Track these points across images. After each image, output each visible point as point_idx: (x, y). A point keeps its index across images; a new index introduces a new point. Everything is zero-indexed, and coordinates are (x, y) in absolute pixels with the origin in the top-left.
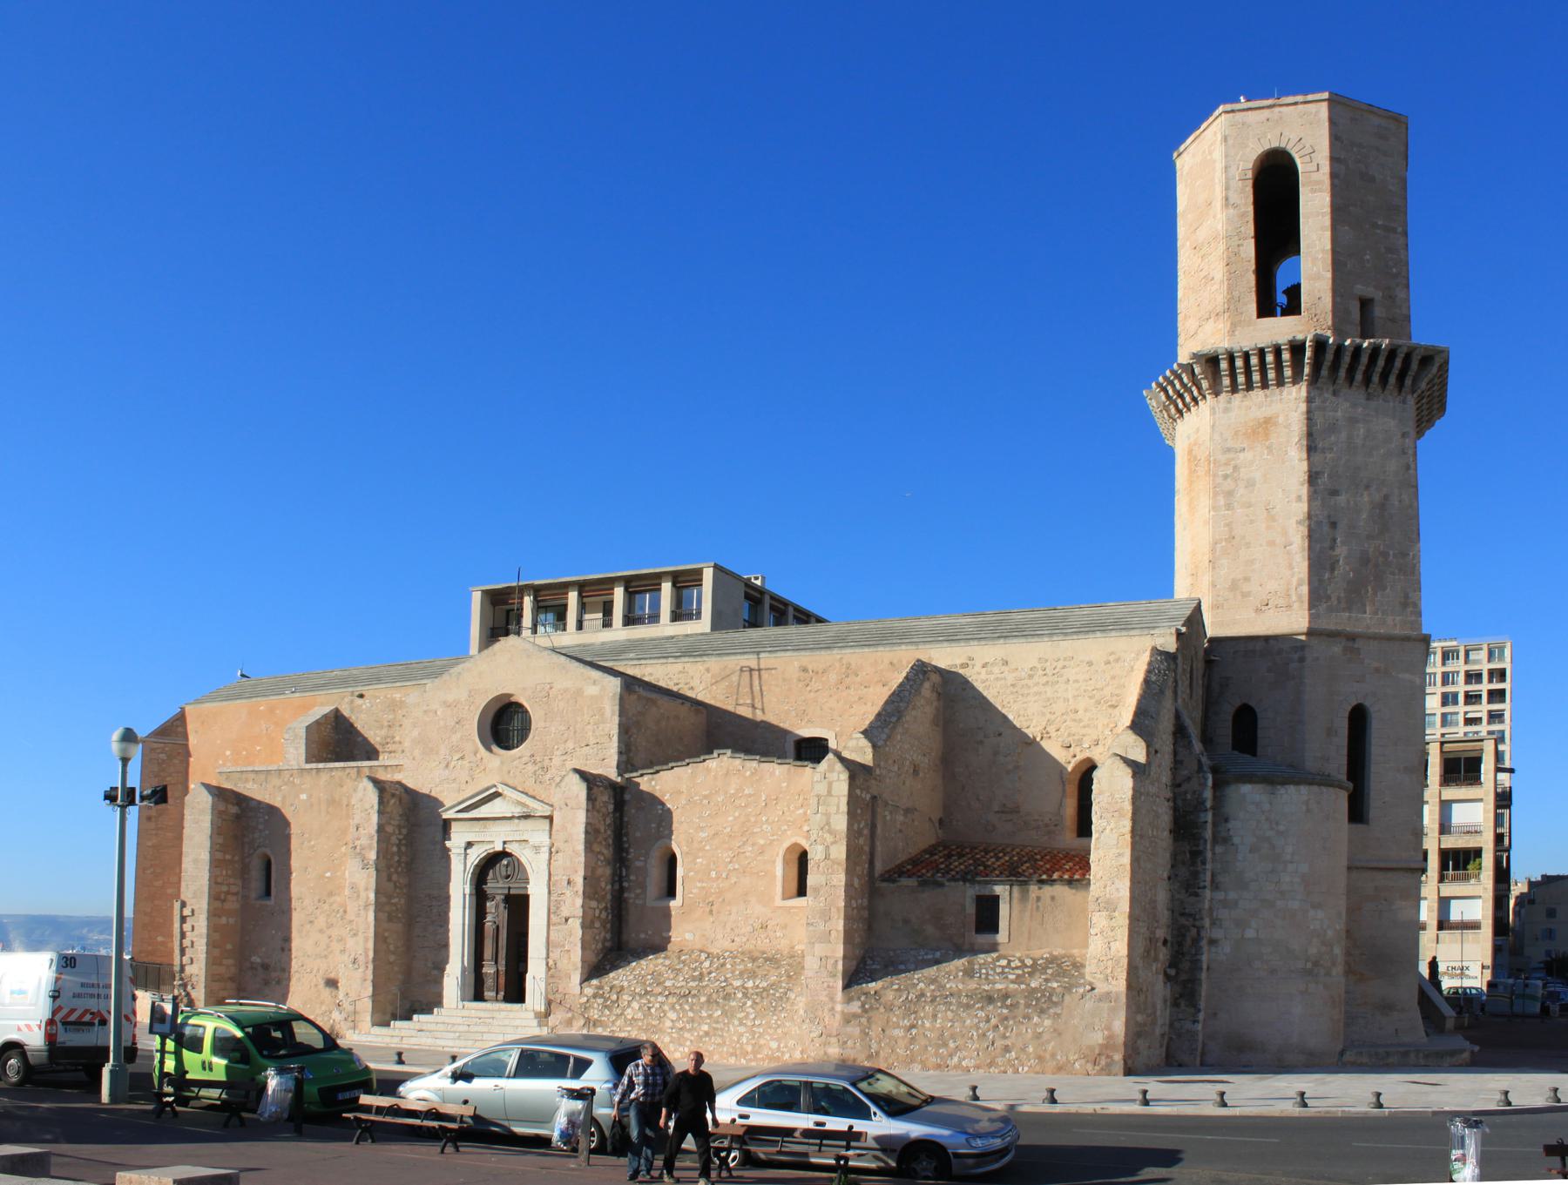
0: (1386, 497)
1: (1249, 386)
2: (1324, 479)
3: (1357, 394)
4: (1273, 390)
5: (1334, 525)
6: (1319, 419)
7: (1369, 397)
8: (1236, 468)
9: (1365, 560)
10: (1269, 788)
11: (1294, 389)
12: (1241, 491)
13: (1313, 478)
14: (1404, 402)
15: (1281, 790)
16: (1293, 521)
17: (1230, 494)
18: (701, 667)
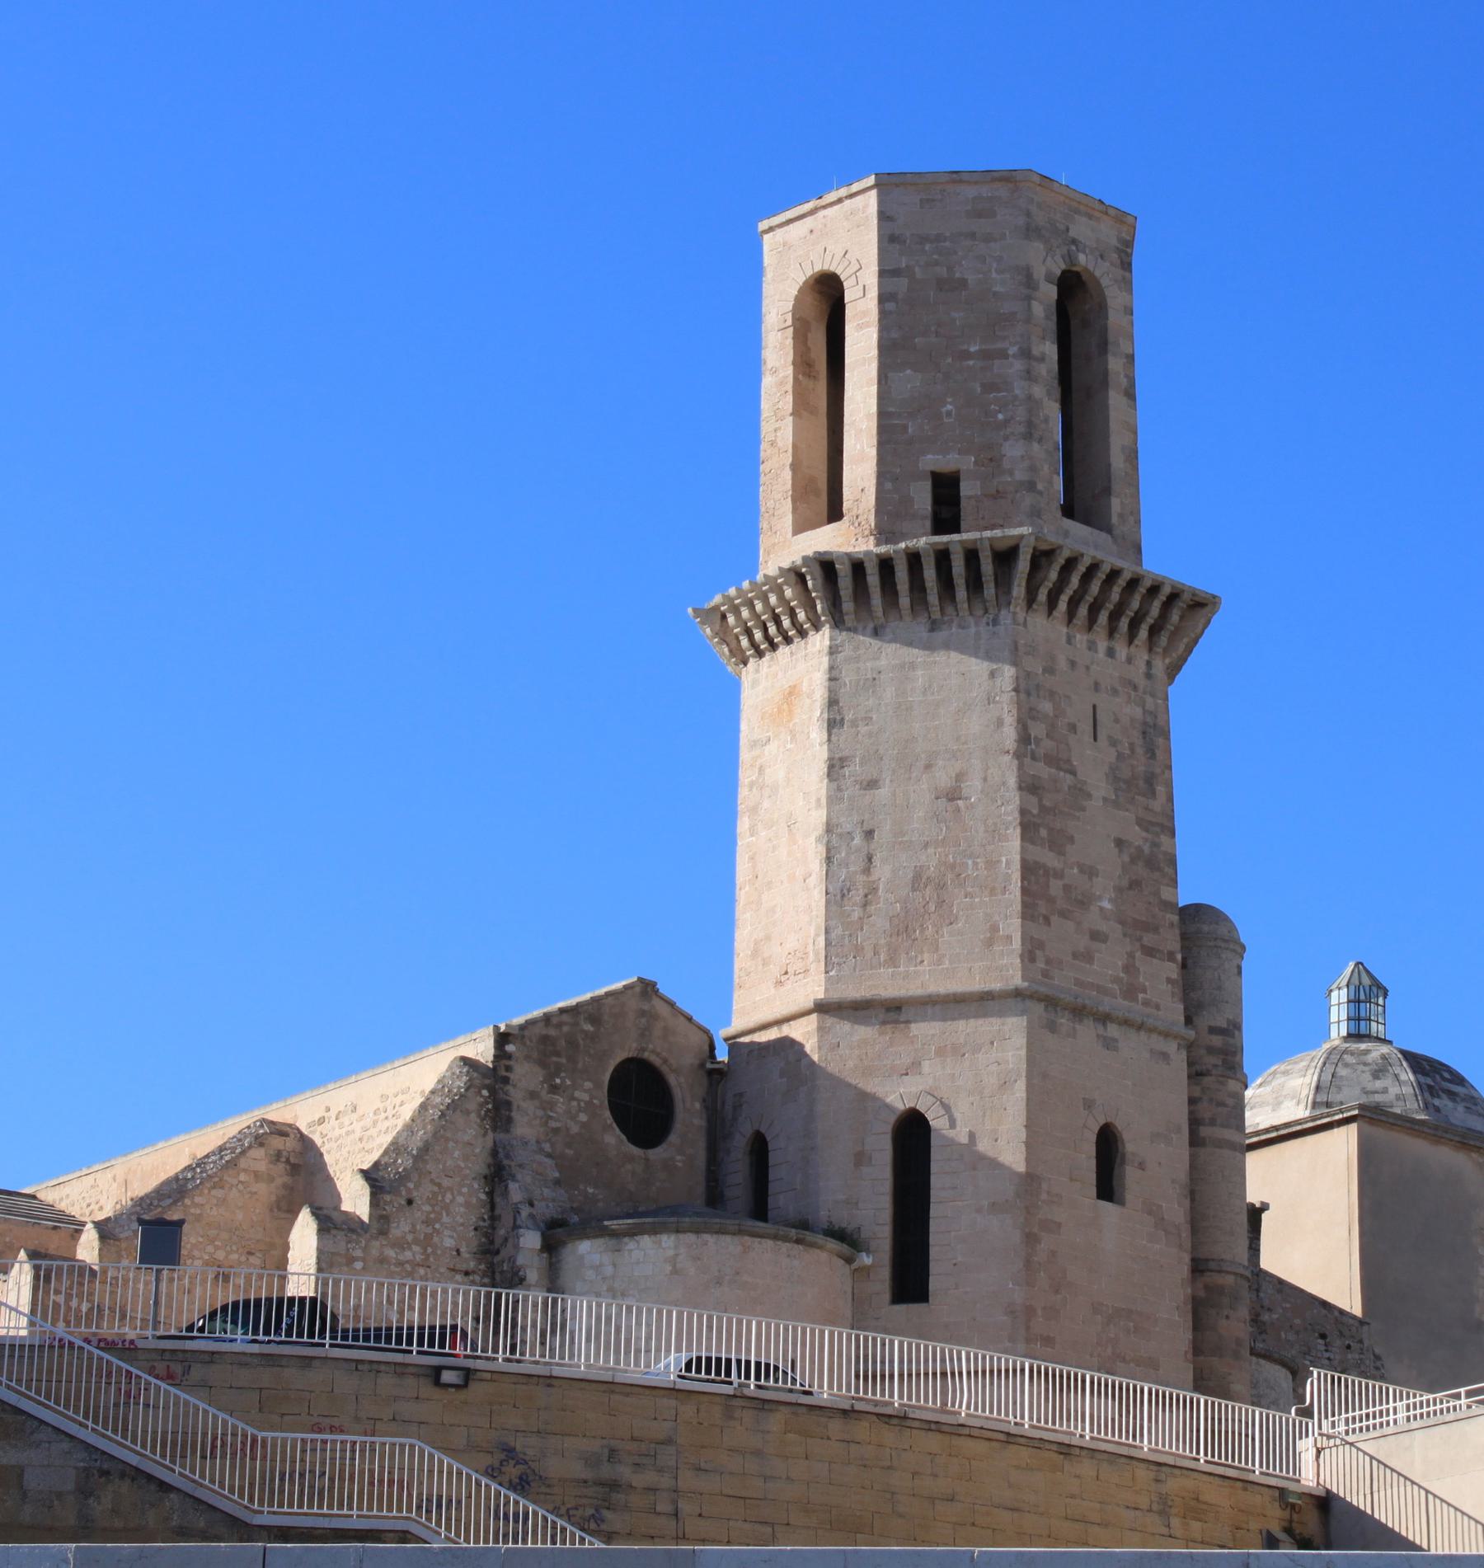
0: (960, 777)
1: (773, 647)
2: (854, 769)
3: (920, 628)
4: (783, 650)
5: (869, 834)
6: (848, 677)
7: (934, 626)
8: (761, 769)
9: (918, 880)
10: (612, 1242)
11: (818, 636)
12: (766, 804)
13: (835, 767)
14: (995, 622)
15: (630, 1244)
16: (813, 839)
17: (754, 810)
18: (109, 1175)
